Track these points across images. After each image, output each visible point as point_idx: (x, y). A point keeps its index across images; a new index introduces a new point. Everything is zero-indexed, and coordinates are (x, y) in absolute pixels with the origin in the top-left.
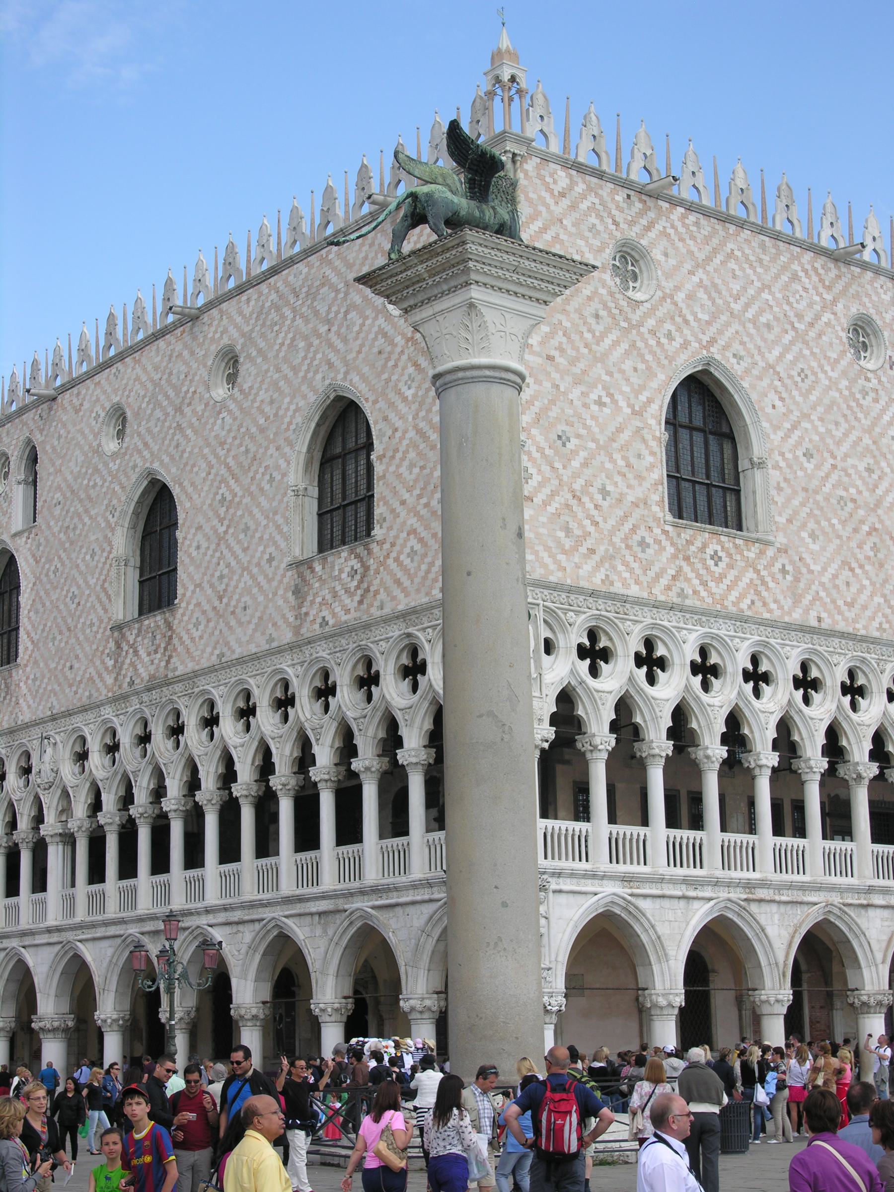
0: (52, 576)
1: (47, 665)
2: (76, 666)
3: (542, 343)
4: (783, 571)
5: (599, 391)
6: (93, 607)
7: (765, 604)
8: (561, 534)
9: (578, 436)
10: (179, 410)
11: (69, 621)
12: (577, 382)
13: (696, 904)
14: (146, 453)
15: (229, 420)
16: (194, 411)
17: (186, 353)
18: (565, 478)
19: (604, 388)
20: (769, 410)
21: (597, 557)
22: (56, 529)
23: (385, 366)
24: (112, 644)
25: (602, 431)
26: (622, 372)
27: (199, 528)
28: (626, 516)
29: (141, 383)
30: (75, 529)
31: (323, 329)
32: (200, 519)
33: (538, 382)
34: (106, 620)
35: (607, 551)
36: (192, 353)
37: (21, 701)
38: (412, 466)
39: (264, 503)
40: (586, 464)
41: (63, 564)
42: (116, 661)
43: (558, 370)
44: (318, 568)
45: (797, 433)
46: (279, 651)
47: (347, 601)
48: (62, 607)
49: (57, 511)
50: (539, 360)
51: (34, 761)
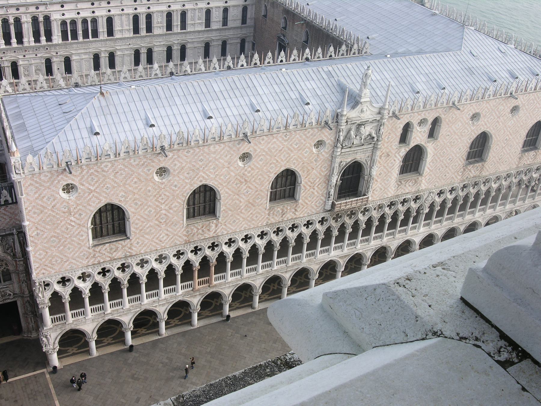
0: (442, 154)
1: (435, 175)
2: (447, 175)
6: (457, 161)
10: (499, 117)
11: (447, 165)
14: (485, 126)
15: (513, 122)
17: (504, 104)
24: (462, 170)
29: (488, 109)
32: (499, 143)
36: (506, 105)
37: (422, 185)
39: (517, 140)
41: (447, 151)
44: (526, 154)
47: (531, 160)
48: (444, 161)
49: (447, 137)
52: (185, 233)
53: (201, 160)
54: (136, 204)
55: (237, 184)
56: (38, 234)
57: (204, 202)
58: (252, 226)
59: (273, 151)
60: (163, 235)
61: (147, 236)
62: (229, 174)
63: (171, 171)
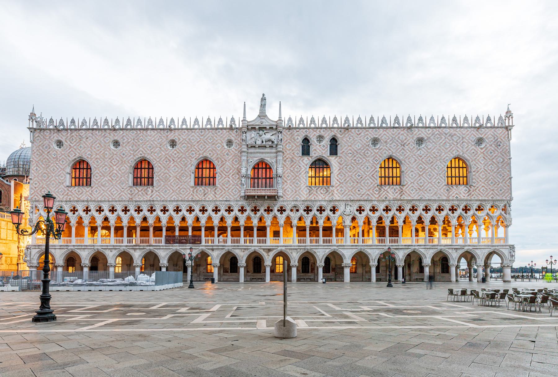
1: (347, 188)
2: (361, 191)
16: (409, 147)
22: (350, 159)
23: (474, 156)
27: (412, 171)
30: (359, 161)
31: (456, 144)
34: (374, 183)
37: (335, 195)
38: (483, 175)
42: (379, 193)
46: (443, 200)
47: (464, 195)
49: (350, 155)
51: (341, 208)
52: (129, 192)
53: (142, 140)
54: (97, 162)
55: (166, 162)
56: (37, 169)
57: (143, 173)
58: (180, 199)
59: (193, 141)
60: (114, 189)
61: (103, 188)
62: (161, 153)
63: (121, 143)
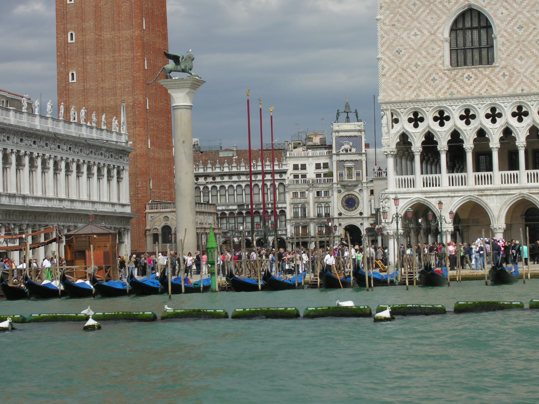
3: (390, 21)
4: (504, 75)
5: (416, 30)
7: (493, 90)
8: (398, 84)
9: (405, 49)
12: (405, 30)
13: (456, 198)
18: (399, 65)
19: (417, 29)
20: (500, 15)
21: (413, 89)
25: (416, 44)
26: (426, 21)
28: (426, 72)
33: (388, 35)
35: (417, 86)
40: (409, 58)
43: (396, 28)
45: (514, 20)
50: (389, 27)
